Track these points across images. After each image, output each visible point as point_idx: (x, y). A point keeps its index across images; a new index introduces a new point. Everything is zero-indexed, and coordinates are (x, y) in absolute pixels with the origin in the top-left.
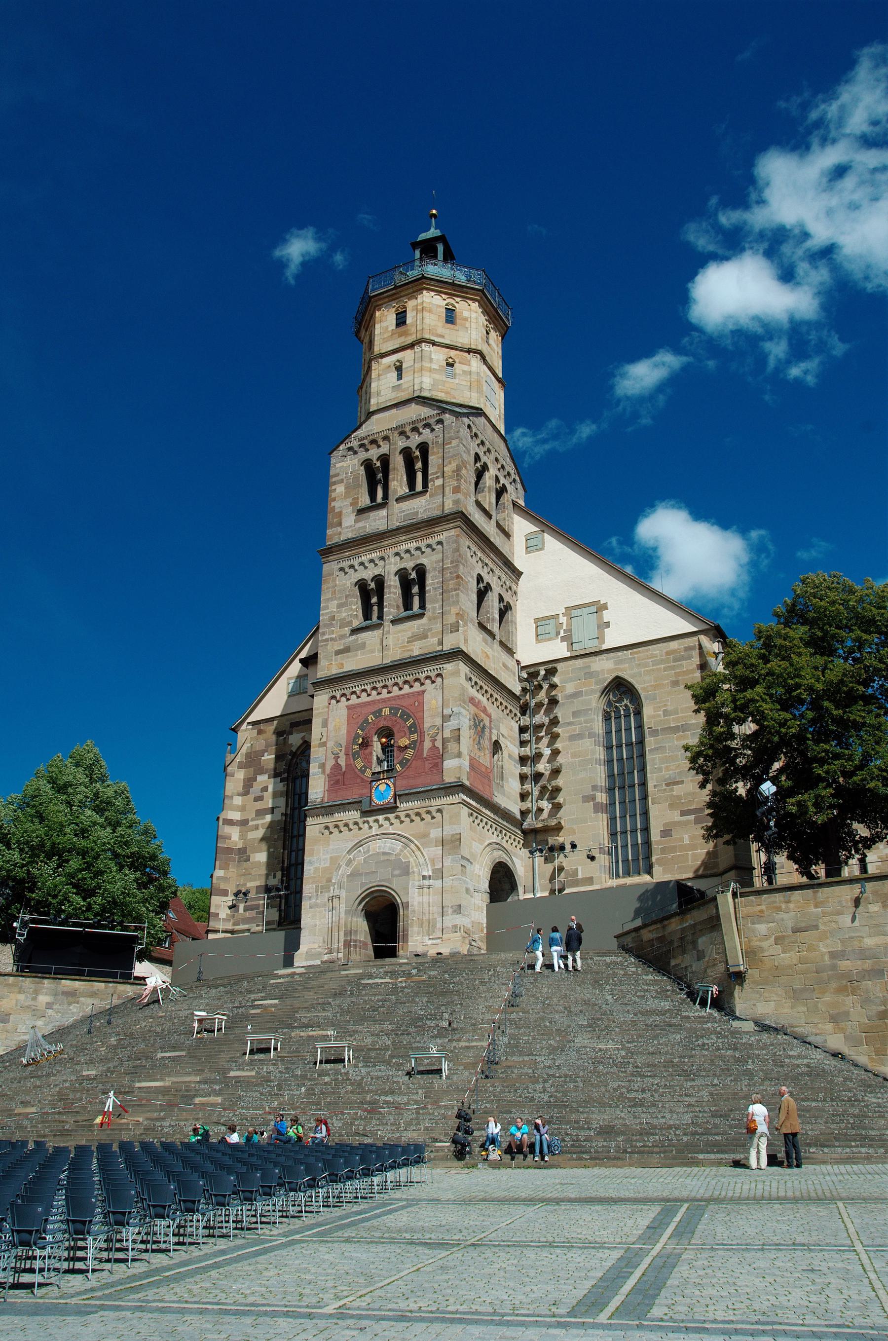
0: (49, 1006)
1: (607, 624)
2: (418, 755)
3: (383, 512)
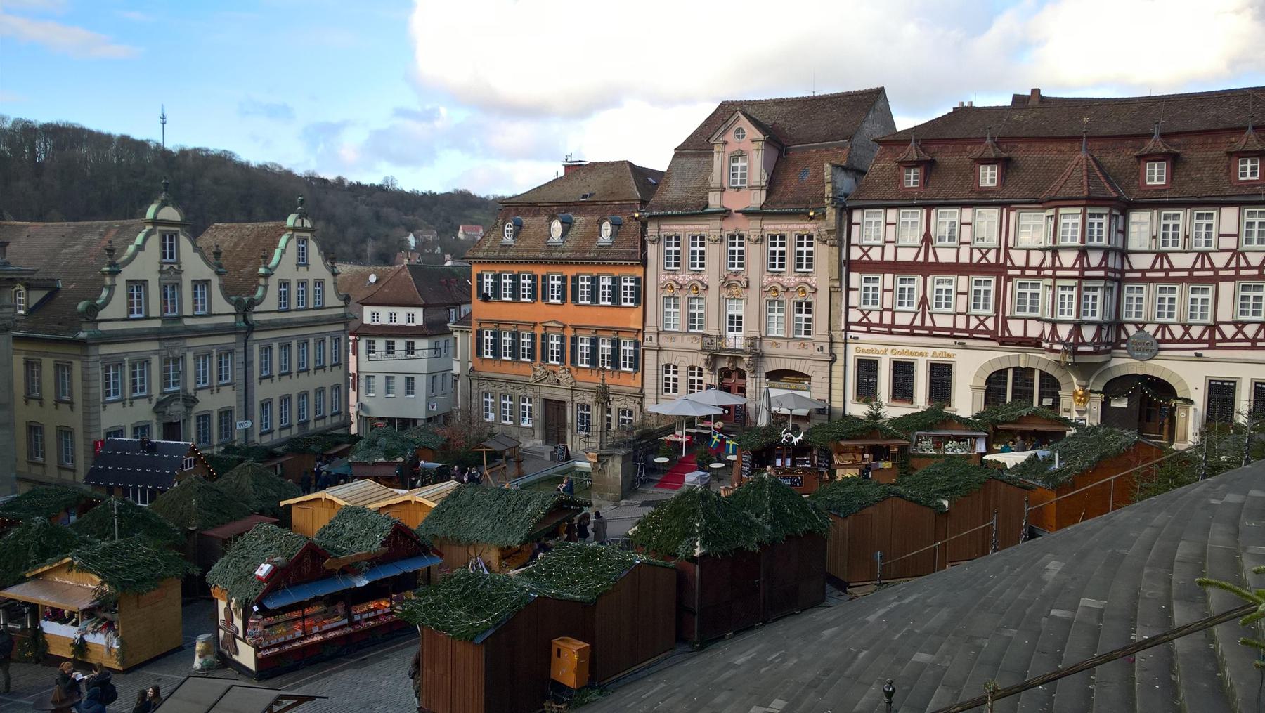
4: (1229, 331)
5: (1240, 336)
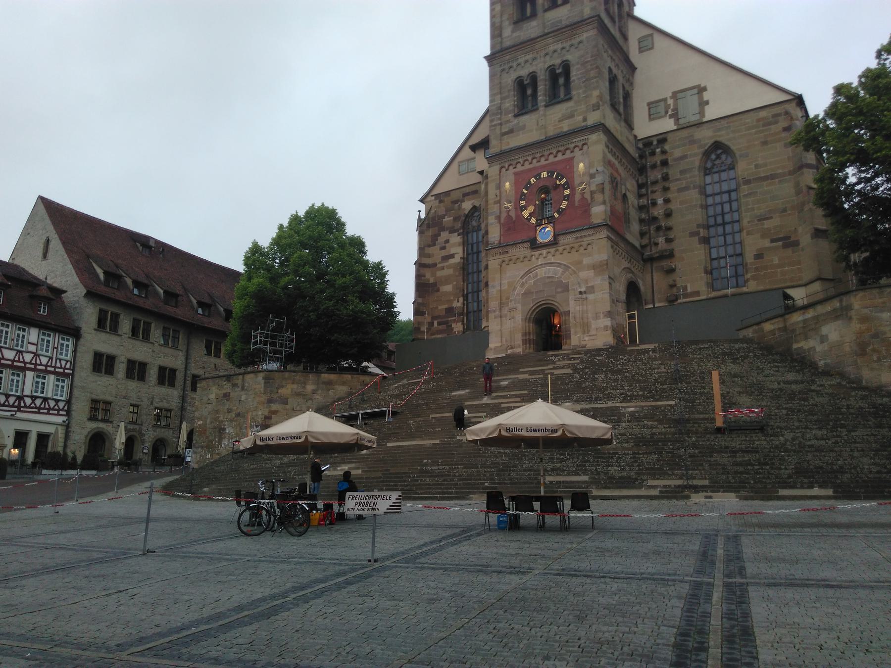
0: (314, 392)
1: (707, 103)
3: (534, 23)
4: (28, 401)
5: (33, 405)
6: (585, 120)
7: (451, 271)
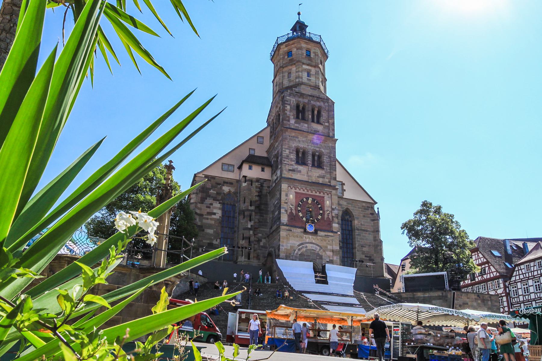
1: (345, 190)
2: (323, 218)
6: (330, 182)
7: (213, 222)
